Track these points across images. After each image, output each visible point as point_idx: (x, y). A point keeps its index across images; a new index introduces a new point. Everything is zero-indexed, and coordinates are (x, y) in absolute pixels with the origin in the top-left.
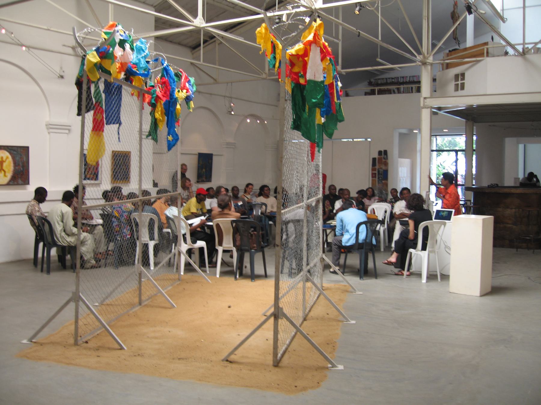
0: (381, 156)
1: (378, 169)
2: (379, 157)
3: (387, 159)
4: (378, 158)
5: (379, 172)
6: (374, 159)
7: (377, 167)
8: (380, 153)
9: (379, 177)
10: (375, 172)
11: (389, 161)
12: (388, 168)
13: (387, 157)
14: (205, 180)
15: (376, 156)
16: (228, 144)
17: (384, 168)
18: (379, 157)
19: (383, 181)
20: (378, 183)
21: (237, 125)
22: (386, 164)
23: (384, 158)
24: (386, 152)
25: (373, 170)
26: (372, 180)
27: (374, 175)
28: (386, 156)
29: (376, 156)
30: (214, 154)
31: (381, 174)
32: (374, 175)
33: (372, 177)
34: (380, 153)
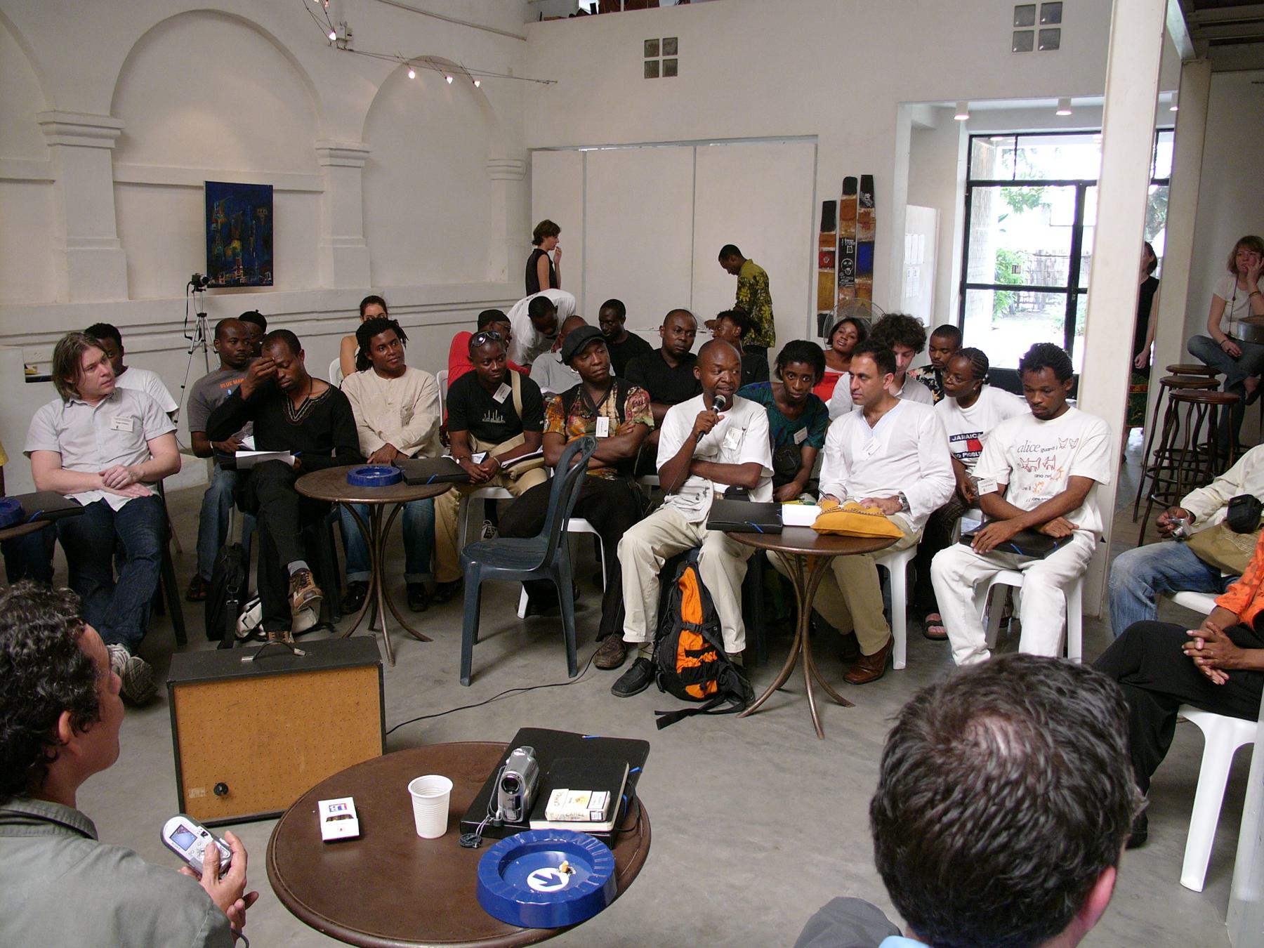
0: (854, 197)
1: (840, 239)
2: (845, 198)
3: (873, 206)
4: (842, 201)
5: (843, 248)
6: (829, 207)
7: (838, 232)
8: (849, 184)
9: (845, 267)
10: (832, 249)
11: (879, 213)
12: (874, 236)
13: (872, 197)
15: (836, 194)
16: (335, 152)
17: (861, 234)
18: (845, 198)
19: (856, 280)
20: (839, 285)
21: (374, 90)
22: (868, 222)
23: (862, 203)
24: (868, 182)
25: (823, 242)
26: (820, 273)
27: (826, 260)
28: (868, 195)
29: (836, 194)
31: (852, 256)
32: (827, 260)
33: (822, 265)
34: (849, 184)
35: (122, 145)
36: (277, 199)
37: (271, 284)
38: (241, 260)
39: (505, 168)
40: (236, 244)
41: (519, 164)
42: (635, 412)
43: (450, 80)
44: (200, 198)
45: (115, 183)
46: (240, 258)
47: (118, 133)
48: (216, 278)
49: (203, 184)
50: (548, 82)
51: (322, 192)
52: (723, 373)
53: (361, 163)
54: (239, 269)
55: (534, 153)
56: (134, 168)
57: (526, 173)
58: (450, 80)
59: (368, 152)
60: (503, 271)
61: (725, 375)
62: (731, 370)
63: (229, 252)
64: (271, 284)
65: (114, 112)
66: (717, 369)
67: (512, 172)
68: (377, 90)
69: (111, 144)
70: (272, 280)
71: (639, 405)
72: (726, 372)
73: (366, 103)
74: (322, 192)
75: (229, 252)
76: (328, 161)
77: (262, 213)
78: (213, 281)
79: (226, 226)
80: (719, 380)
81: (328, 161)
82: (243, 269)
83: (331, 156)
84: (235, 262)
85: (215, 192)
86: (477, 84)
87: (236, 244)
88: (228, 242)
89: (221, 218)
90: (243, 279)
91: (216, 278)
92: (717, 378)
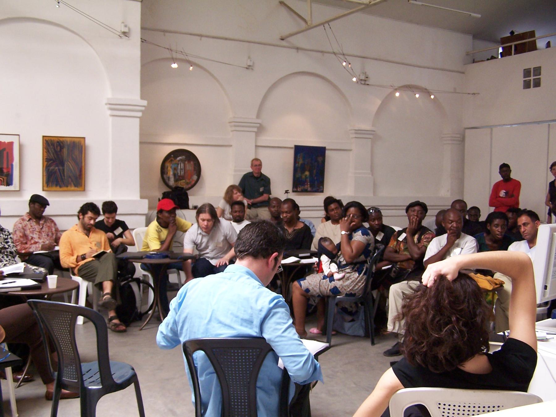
14: (309, 189)
21: (379, 102)
30: (327, 148)
35: (260, 130)
36: (327, 153)
37: (322, 192)
38: (309, 181)
39: (450, 138)
40: (307, 173)
41: (458, 136)
42: (425, 242)
43: (417, 96)
44: (292, 153)
45: (257, 146)
46: (308, 180)
47: (258, 125)
48: (297, 188)
49: (293, 146)
50: (474, 94)
51: (350, 150)
52: (453, 223)
53: (371, 136)
54: (307, 184)
55: (467, 131)
56: (264, 140)
57: (462, 140)
58: (417, 96)
59: (374, 131)
60: (448, 191)
61: (454, 224)
62: (456, 222)
63: (304, 177)
64: (322, 192)
65: (258, 116)
66: (450, 222)
67: (454, 140)
68: (380, 102)
69: (255, 130)
70: (323, 190)
71: (427, 238)
72: (455, 223)
73: (374, 109)
74: (350, 150)
75: (304, 177)
76: (354, 136)
77: (320, 159)
78: (295, 189)
79: (303, 165)
80: (451, 226)
81: (354, 136)
82: (310, 184)
83: (356, 133)
84: (306, 181)
85: (299, 150)
86: (432, 97)
87: (307, 173)
88: (303, 171)
89: (301, 161)
90: (309, 189)
91: (297, 188)
92: (450, 226)
